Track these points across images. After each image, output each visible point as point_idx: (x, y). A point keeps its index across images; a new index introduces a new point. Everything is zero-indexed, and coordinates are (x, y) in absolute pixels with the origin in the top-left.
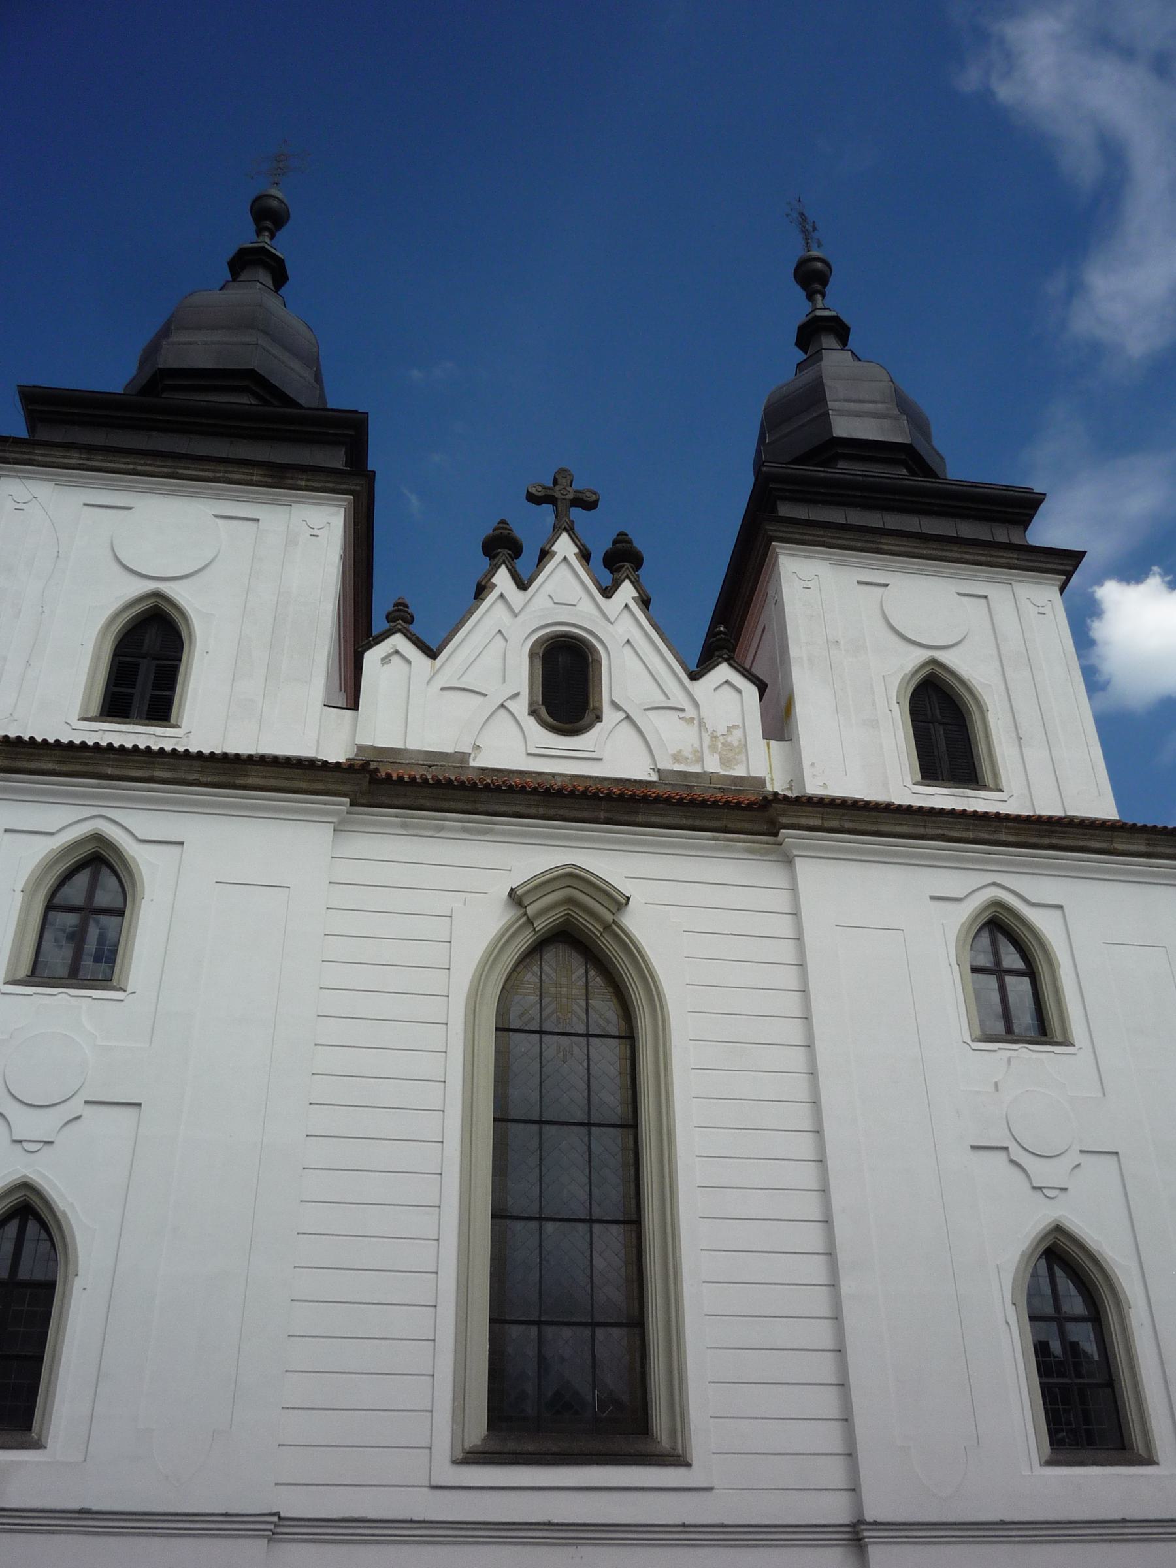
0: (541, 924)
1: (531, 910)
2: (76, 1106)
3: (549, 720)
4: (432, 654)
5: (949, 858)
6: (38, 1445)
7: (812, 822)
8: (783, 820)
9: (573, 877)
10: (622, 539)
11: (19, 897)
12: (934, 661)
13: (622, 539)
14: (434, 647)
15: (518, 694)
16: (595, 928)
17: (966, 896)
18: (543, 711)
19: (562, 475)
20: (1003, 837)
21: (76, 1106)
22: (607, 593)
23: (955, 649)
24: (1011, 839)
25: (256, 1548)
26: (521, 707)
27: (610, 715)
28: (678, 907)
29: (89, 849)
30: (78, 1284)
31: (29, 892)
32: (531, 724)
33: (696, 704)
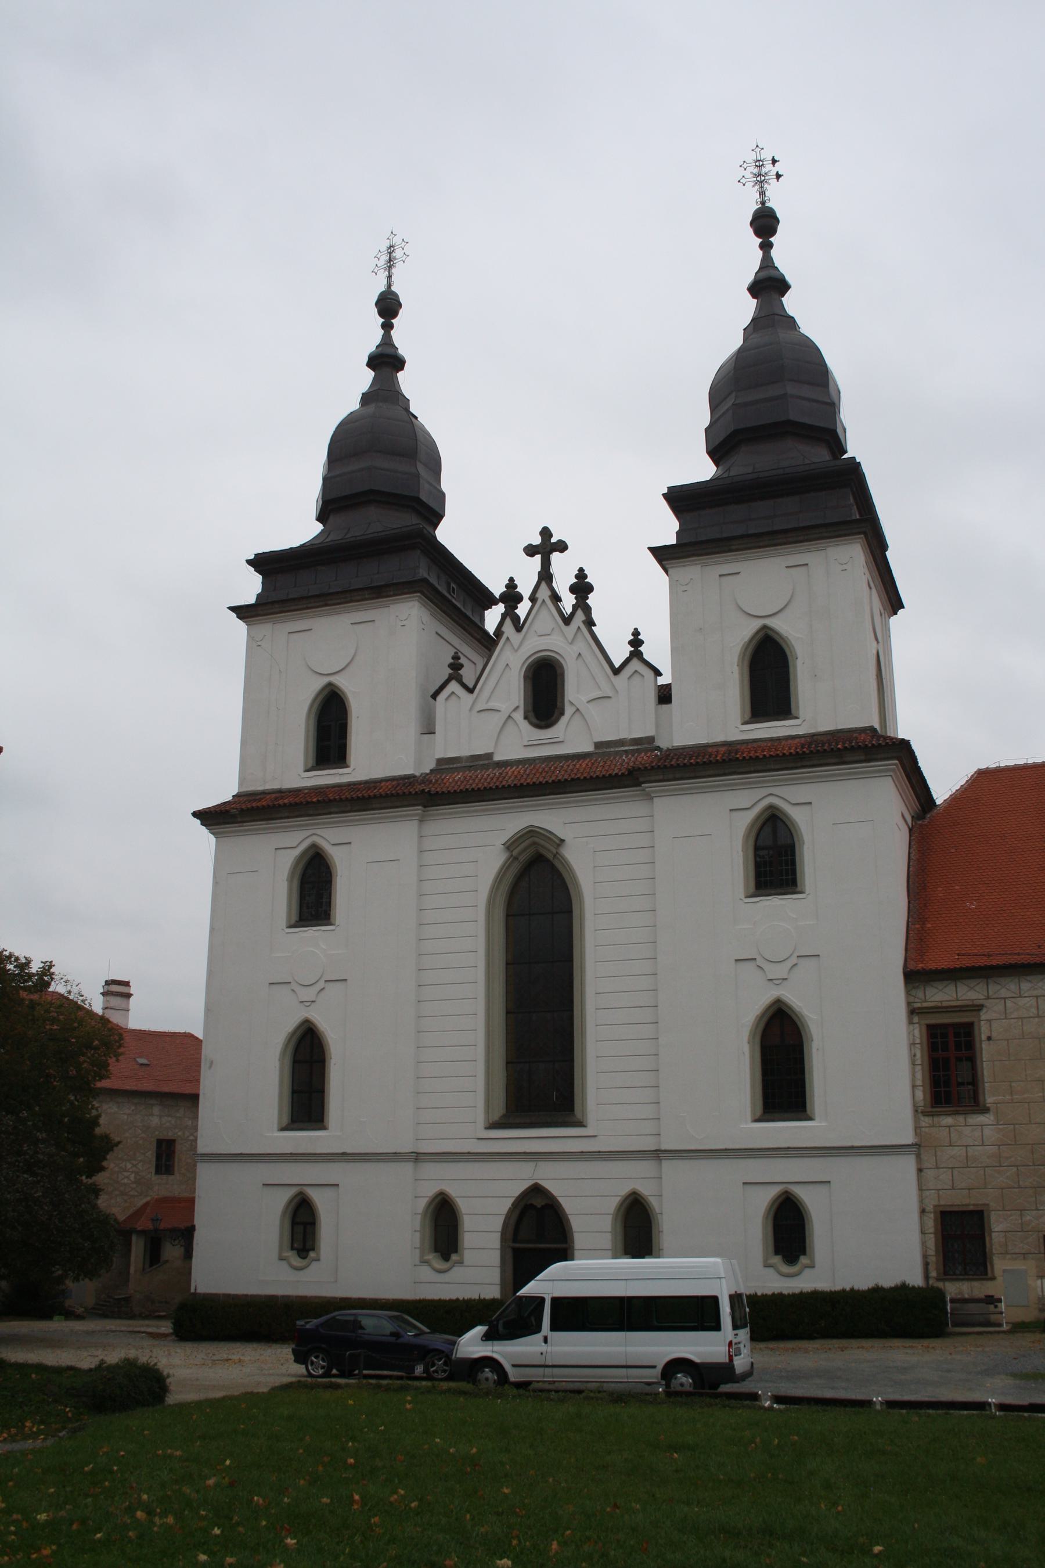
0: (522, 858)
1: (515, 853)
2: (321, 984)
3: (535, 721)
4: (471, 691)
5: (742, 784)
6: (325, 1128)
7: (657, 778)
8: (641, 779)
9: (531, 833)
10: (581, 575)
11: (286, 883)
12: (765, 627)
13: (581, 575)
14: (471, 686)
15: (517, 707)
16: (550, 857)
17: (752, 806)
18: (531, 715)
19: (546, 533)
20: (773, 767)
21: (321, 984)
22: (567, 620)
23: (780, 615)
24: (777, 767)
25: (408, 1168)
26: (519, 716)
27: (569, 710)
28: (591, 838)
29: (311, 853)
30: (333, 1062)
31: (290, 880)
32: (525, 725)
33: (617, 692)
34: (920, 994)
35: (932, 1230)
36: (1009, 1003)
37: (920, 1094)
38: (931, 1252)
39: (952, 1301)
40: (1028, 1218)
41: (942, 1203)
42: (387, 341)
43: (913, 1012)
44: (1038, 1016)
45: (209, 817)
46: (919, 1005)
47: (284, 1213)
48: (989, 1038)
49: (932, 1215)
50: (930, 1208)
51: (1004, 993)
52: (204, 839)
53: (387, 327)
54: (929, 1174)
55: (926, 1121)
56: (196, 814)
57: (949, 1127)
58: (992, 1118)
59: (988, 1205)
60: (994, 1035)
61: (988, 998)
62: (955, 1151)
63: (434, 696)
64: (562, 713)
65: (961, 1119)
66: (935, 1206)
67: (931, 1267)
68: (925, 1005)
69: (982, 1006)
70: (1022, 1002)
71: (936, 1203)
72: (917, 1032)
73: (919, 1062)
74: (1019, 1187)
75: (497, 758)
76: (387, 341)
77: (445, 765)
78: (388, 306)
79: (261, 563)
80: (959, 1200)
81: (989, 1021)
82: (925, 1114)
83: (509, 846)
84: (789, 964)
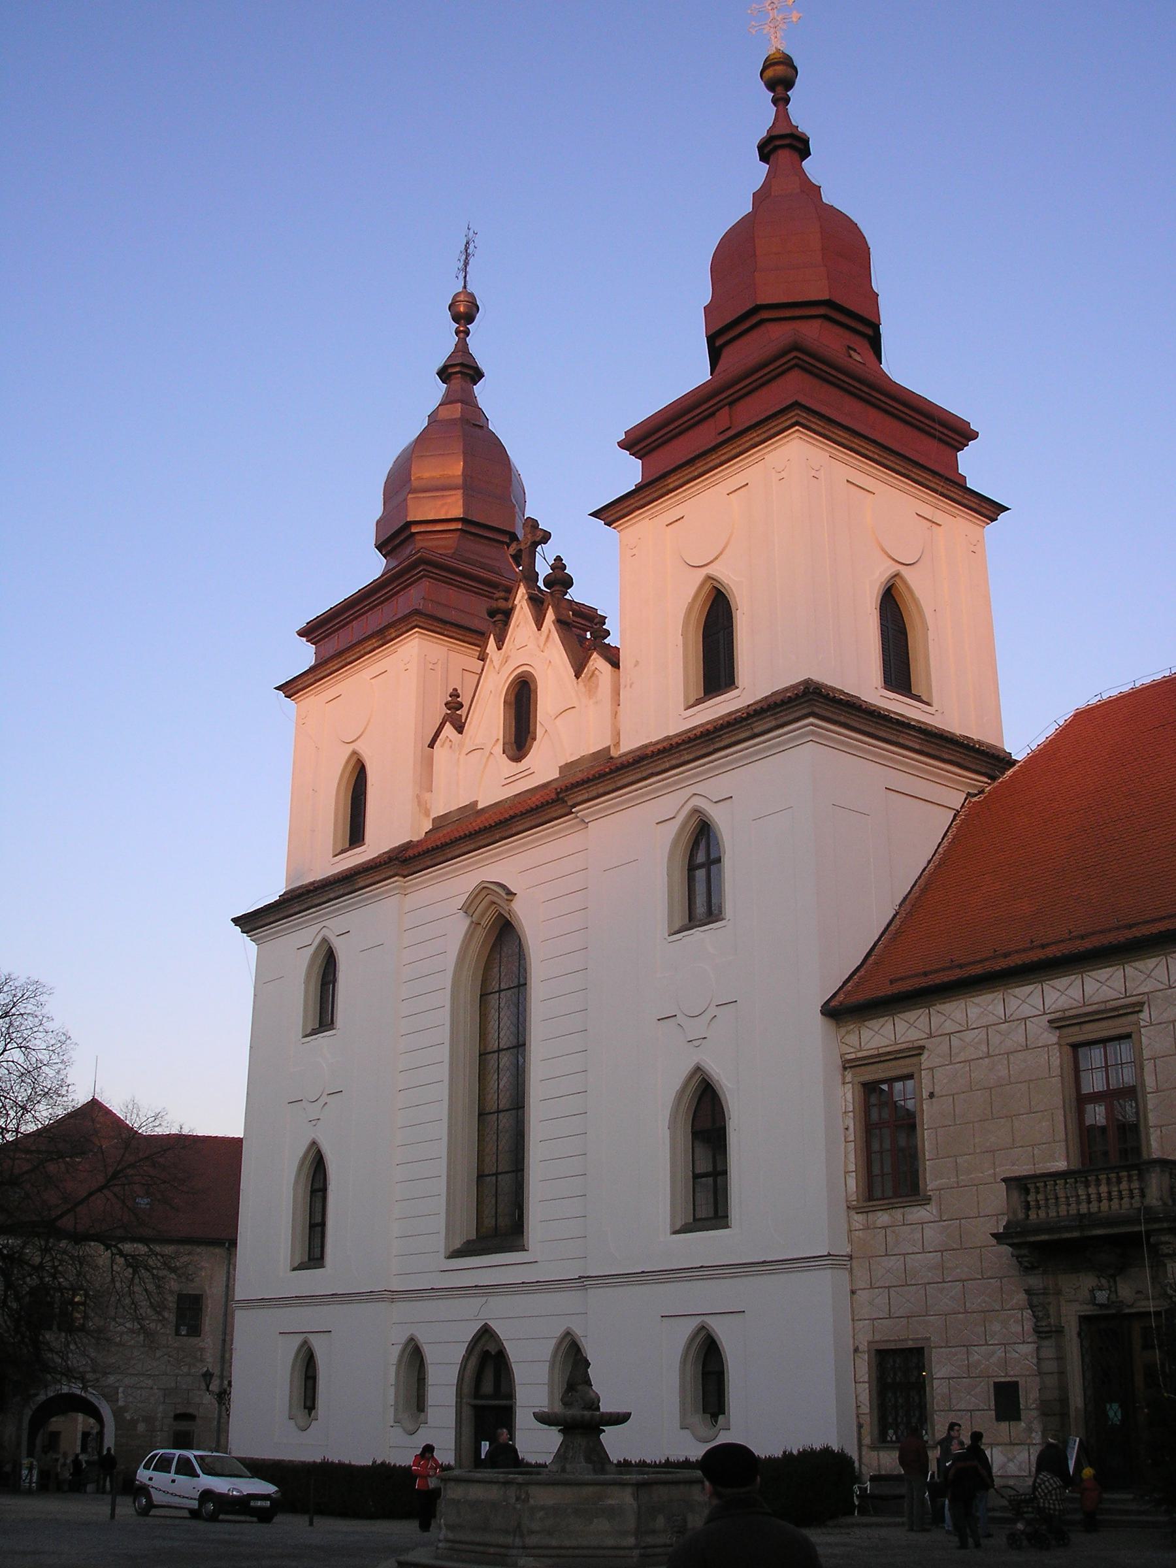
9: (484, 889)
26: (499, 748)
34: (852, 1039)
35: (866, 1378)
36: (955, 1041)
37: (852, 1183)
38: (865, 1409)
39: (873, 1479)
40: (976, 1357)
41: (877, 1338)
42: (462, 348)
43: (848, 1065)
44: (988, 1056)
45: (249, 923)
46: (853, 1056)
47: (684, 1361)
48: (932, 1095)
49: (866, 1357)
50: (864, 1347)
51: (949, 1027)
52: (245, 948)
53: (463, 334)
54: (863, 1296)
55: (859, 1219)
56: (236, 921)
57: (885, 1228)
58: (934, 1211)
59: (928, 1339)
60: (937, 1090)
61: (931, 1036)
62: (892, 1262)
63: (431, 745)
64: (534, 739)
65: (898, 1214)
66: (869, 1343)
67: (866, 1430)
68: (860, 1055)
69: (922, 1048)
70: (969, 1036)
71: (871, 1339)
72: (849, 1096)
73: (852, 1138)
74: (966, 1312)
75: (480, 807)
76: (462, 348)
77: (440, 822)
78: (464, 313)
79: (310, 632)
80: (898, 1334)
81: (932, 1069)
82: (859, 1210)
83: (467, 909)
84: (707, 1016)
